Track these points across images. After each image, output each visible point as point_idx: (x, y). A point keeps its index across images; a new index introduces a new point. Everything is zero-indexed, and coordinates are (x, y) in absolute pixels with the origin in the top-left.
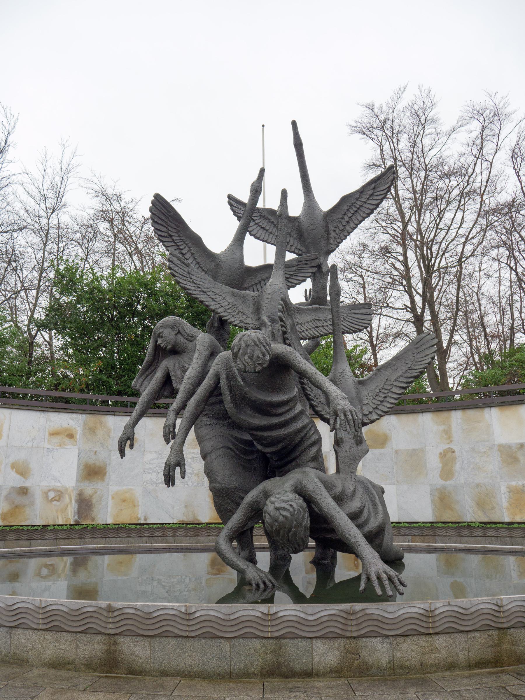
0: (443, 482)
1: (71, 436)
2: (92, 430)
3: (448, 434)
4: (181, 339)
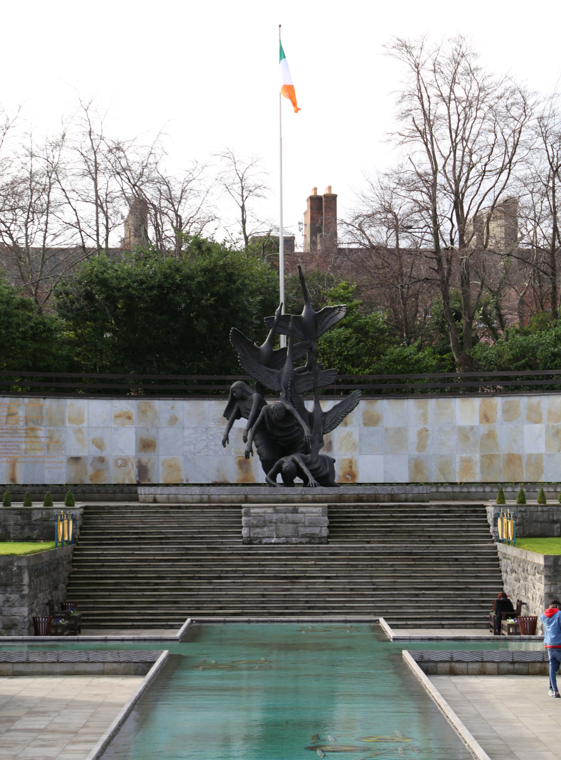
0: (419, 453)
1: (129, 418)
2: (143, 413)
3: (425, 416)
4: (245, 394)
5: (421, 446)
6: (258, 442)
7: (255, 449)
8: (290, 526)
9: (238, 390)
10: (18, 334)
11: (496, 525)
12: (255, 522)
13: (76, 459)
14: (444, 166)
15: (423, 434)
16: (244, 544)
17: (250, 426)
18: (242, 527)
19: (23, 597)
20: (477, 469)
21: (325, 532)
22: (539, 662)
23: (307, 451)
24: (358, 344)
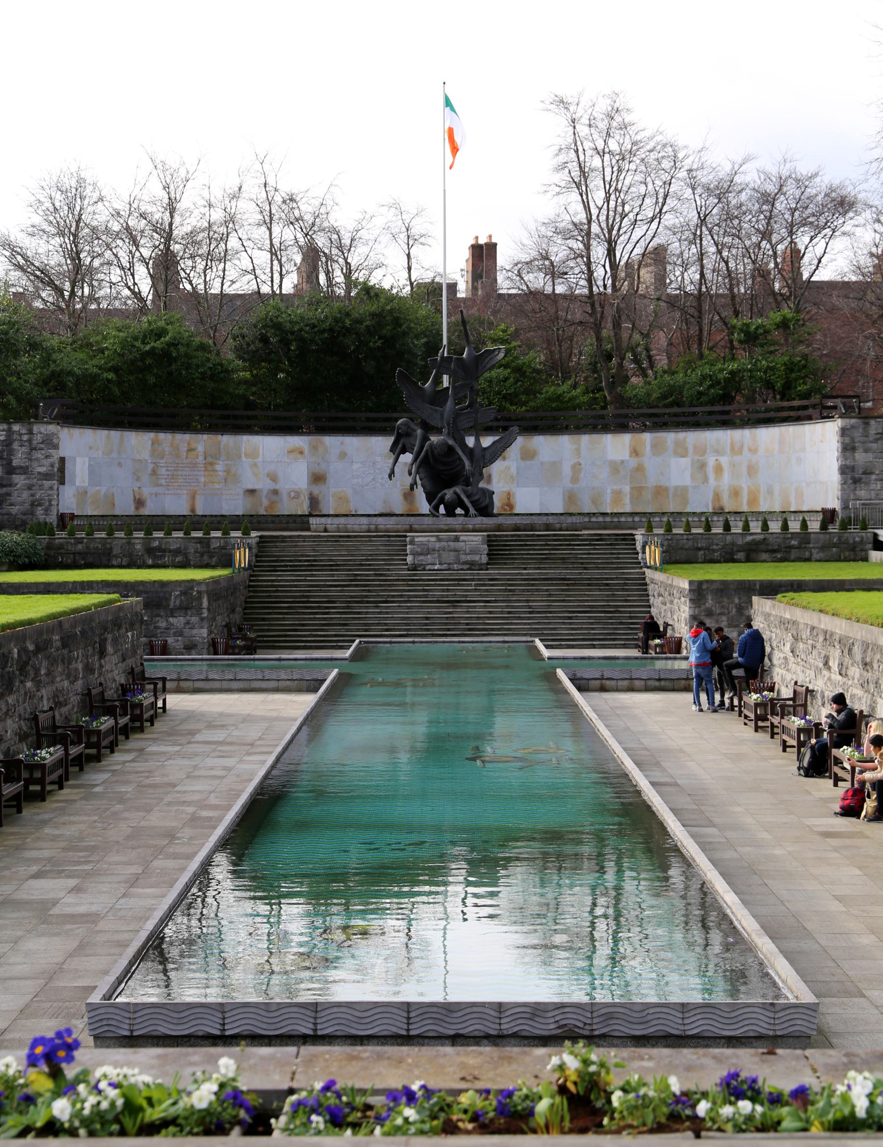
1: (301, 453)
2: (314, 448)
3: (578, 451)
5: (575, 479)
6: (422, 475)
7: (419, 482)
8: (452, 553)
9: (403, 427)
10: (197, 375)
11: (644, 552)
12: (419, 550)
13: (252, 492)
14: (598, 216)
15: (576, 468)
16: (409, 570)
17: (415, 460)
18: (407, 555)
19: (202, 619)
20: (627, 500)
21: (484, 559)
22: (683, 679)
23: (467, 484)
24: (516, 383)
